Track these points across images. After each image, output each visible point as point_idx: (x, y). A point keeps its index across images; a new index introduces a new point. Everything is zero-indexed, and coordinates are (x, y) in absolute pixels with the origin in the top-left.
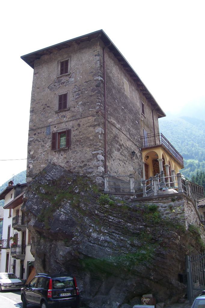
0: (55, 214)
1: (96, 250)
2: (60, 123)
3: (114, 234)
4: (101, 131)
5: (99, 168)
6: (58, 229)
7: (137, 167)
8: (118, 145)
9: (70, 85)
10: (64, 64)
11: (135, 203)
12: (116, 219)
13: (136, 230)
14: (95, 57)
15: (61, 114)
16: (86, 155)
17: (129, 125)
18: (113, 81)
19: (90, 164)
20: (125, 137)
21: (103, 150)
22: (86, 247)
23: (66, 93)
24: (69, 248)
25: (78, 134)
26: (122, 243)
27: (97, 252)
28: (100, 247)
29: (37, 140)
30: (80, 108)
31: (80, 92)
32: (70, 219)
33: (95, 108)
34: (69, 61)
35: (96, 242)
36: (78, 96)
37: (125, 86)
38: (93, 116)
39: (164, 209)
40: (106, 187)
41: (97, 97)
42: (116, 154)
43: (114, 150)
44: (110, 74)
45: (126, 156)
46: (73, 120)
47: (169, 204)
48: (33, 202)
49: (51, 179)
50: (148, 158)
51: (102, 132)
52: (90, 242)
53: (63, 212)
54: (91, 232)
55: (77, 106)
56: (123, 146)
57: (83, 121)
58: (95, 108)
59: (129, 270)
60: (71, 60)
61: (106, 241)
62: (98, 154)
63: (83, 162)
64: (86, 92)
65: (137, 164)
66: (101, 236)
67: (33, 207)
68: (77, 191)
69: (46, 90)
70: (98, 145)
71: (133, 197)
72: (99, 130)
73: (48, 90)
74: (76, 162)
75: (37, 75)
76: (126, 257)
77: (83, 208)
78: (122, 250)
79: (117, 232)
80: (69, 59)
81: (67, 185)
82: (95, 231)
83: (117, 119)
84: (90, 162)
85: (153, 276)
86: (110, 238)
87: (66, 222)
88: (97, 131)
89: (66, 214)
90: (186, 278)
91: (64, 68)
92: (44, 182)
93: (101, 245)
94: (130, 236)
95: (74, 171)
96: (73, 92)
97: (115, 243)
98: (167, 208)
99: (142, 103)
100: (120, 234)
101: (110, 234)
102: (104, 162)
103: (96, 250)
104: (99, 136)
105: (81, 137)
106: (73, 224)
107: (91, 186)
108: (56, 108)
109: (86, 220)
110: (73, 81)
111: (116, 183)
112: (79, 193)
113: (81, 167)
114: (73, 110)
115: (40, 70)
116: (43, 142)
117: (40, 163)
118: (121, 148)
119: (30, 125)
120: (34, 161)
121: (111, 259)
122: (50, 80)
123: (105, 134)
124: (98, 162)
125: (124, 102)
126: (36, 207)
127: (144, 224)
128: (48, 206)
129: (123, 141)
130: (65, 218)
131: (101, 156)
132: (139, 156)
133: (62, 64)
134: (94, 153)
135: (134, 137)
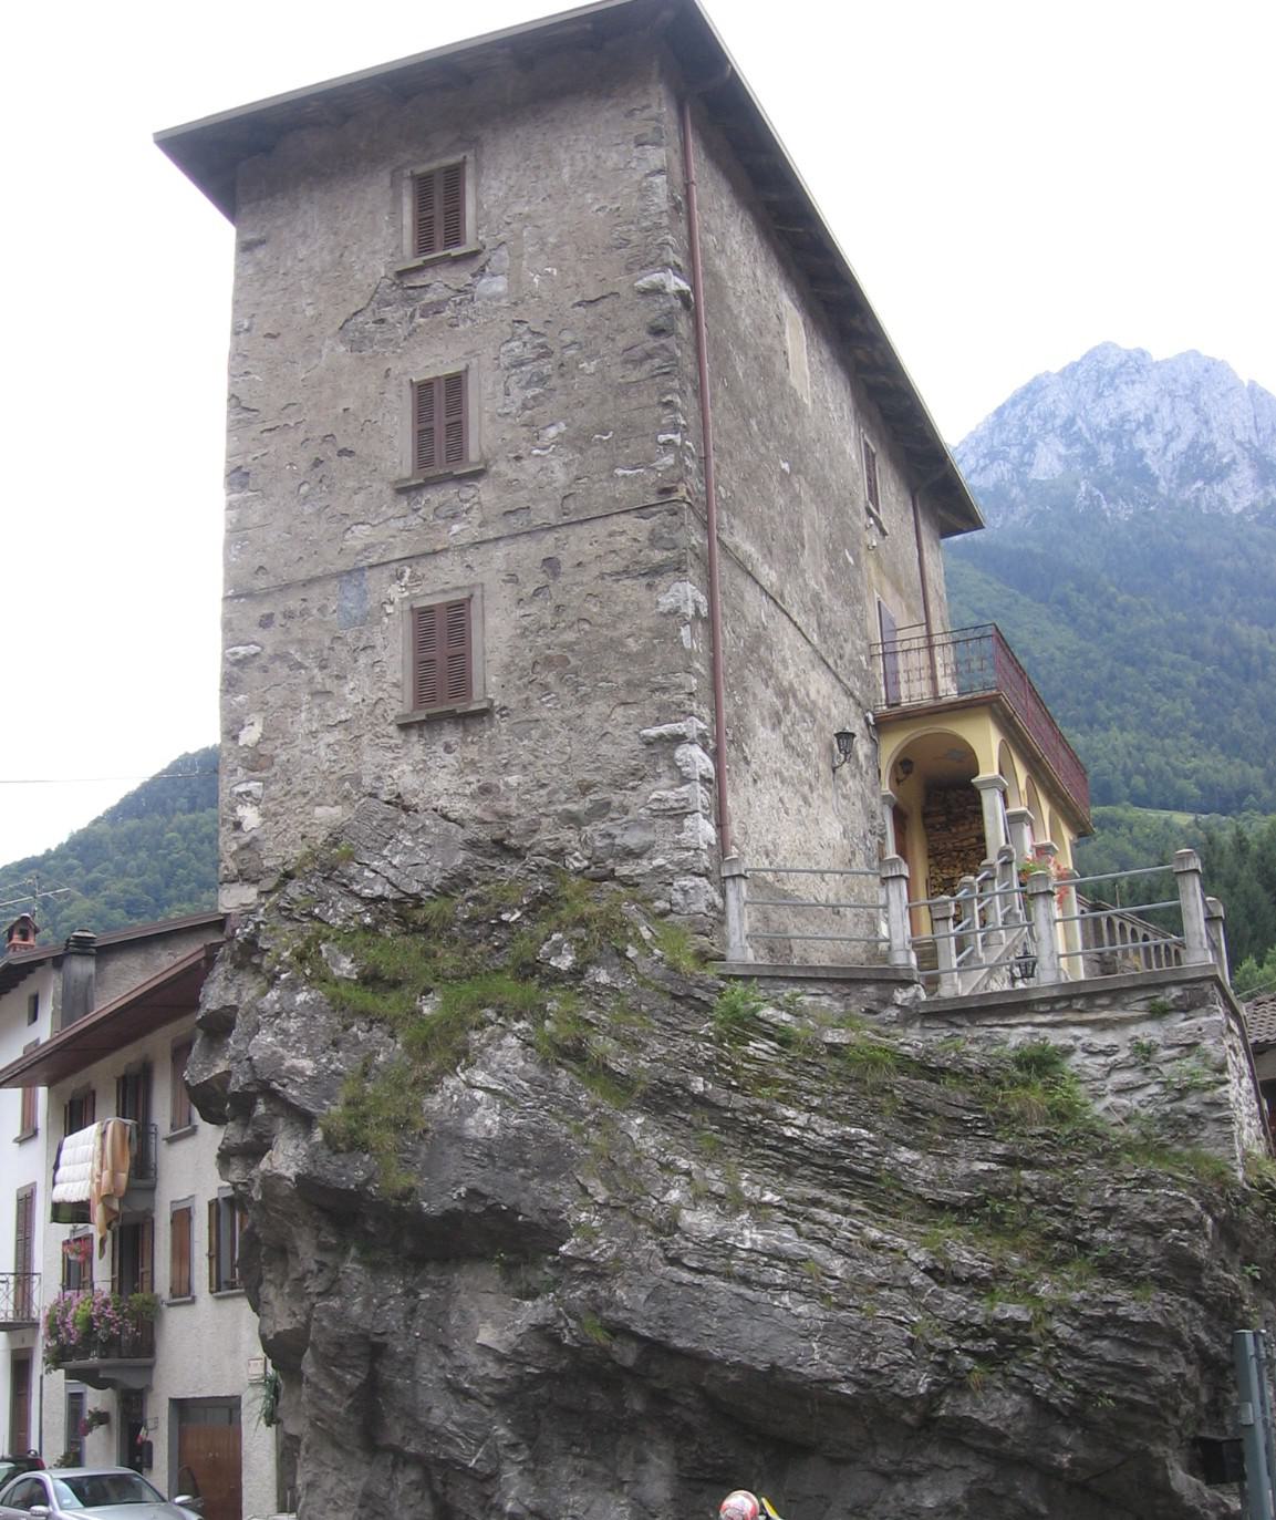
0: (434, 1103)
1: (718, 1313)
2: (425, 555)
3: (823, 1215)
4: (690, 603)
5: (687, 822)
6: (463, 1190)
7: (861, 824)
8: (770, 691)
9: (481, 320)
10: (439, 191)
11: (922, 1027)
12: (822, 1127)
13: (950, 1186)
14: (636, 152)
15: (434, 496)
16: (605, 748)
17: (815, 576)
18: (732, 300)
19: (631, 799)
20: (800, 642)
21: (708, 719)
22: (656, 1294)
23: (460, 367)
24: (539, 1302)
25: (548, 620)
26: (878, 1264)
27: (722, 1318)
28: (743, 1290)
29: (281, 657)
30: (556, 464)
31: (547, 367)
32: (532, 1131)
33: (647, 463)
34: (469, 171)
35: (713, 1264)
36: (538, 390)
37: (787, 336)
38: (642, 511)
39: (1101, 1060)
40: (734, 939)
41: (663, 395)
42: (764, 740)
43: (757, 722)
44: (717, 262)
45: (809, 754)
46: (514, 536)
47: (1133, 1031)
48: (285, 1032)
49: (388, 892)
50: (907, 773)
51: (697, 610)
52: (675, 1261)
53: (487, 1090)
54: (678, 1207)
55: (536, 452)
56: (795, 696)
57: (580, 543)
58: (647, 463)
59: (928, 1422)
60: (479, 170)
61: (776, 1256)
62: (679, 739)
63: (585, 788)
64: (589, 367)
65: (859, 804)
66: (743, 1227)
67: (287, 1064)
68: (565, 962)
69: (325, 351)
70: (680, 687)
71: (911, 991)
72: (685, 593)
73: (342, 349)
74: (543, 792)
75: (260, 253)
76: (911, 1343)
77: (613, 1065)
78: (884, 1304)
79: (838, 1201)
80: (470, 158)
81: (493, 927)
82: (702, 1196)
83: (761, 536)
84: (633, 788)
85: (1068, 1449)
86: (800, 1235)
87: (507, 1152)
88: (667, 602)
89: (505, 1099)
90: (1240, 1457)
91: (439, 216)
92: (340, 910)
93: (745, 1280)
94: (920, 1222)
95: (527, 845)
96: (505, 361)
97: (837, 1265)
98: (1120, 1057)
99: (867, 445)
100: (858, 1212)
101: (794, 1213)
102: (716, 785)
103: (718, 1313)
104: (685, 632)
105: (570, 636)
106: (556, 1162)
107: (646, 935)
108: (399, 455)
109: (635, 1136)
110: (497, 297)
111: (774, 917)
112: (577, 973)
113: (573, 820)
114: (511, 475)
115: (280, 222)
116: (323, 668)
117: (305, 794)
118: (786, 709)
119: (228, 566)
120: (266, 783)
121: (817, 1357)
122: (351, 289)
123: (710, 622)
124: (683, 789)
125: (789, 431)
126: (306, 1064)
127: (1000, 1149)
128: (381, 1058)
129: (792, 669)
130: (505, 1127)
131: (701, 753)
132: (866, 756)
133: (423, 186)
134: (653, 732)
135: (842, 647)
